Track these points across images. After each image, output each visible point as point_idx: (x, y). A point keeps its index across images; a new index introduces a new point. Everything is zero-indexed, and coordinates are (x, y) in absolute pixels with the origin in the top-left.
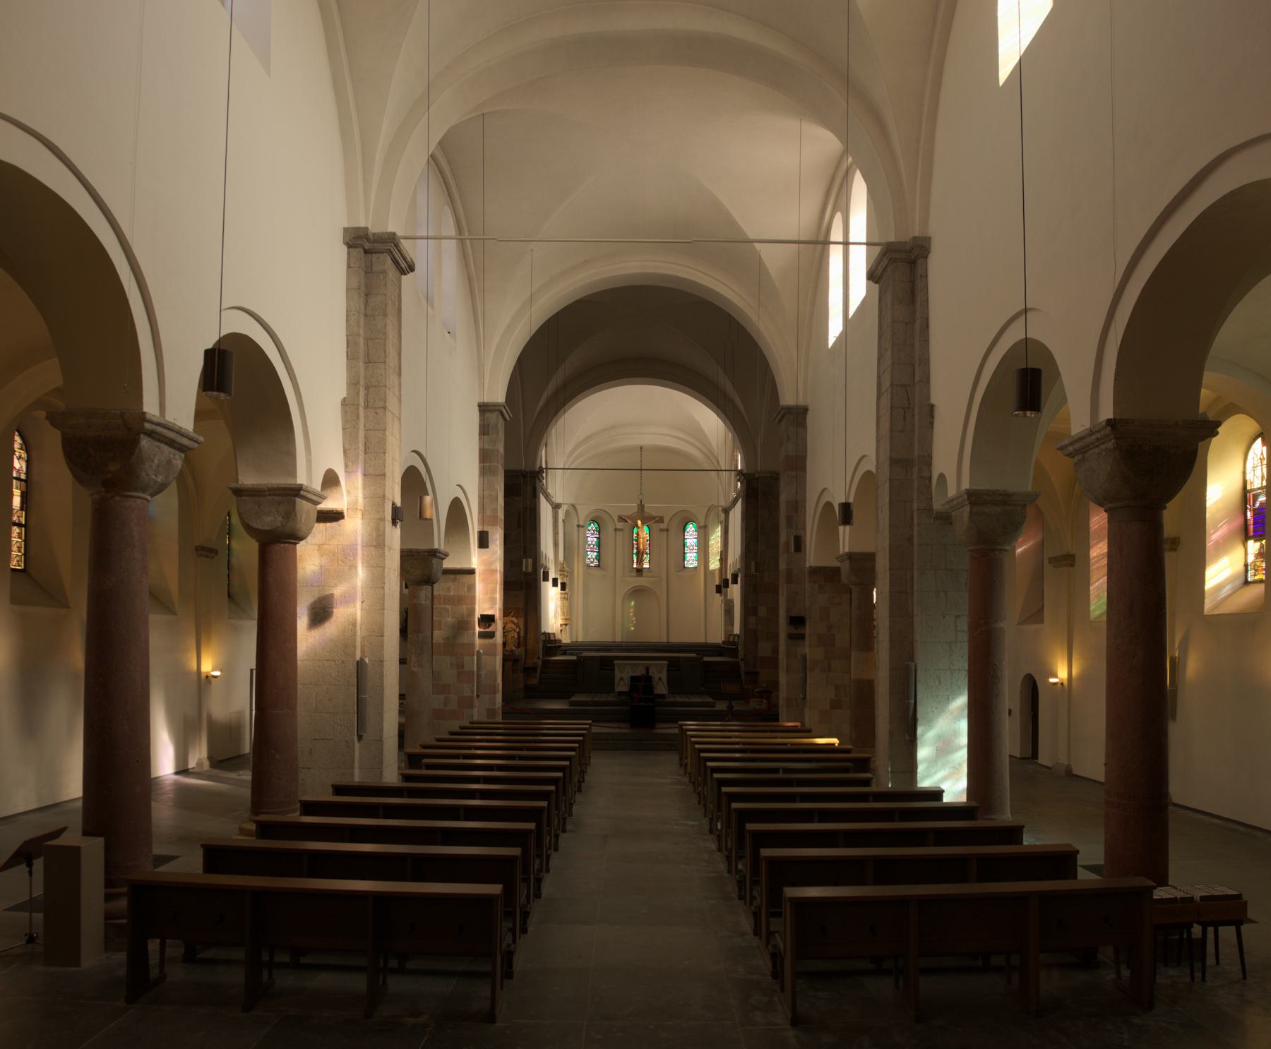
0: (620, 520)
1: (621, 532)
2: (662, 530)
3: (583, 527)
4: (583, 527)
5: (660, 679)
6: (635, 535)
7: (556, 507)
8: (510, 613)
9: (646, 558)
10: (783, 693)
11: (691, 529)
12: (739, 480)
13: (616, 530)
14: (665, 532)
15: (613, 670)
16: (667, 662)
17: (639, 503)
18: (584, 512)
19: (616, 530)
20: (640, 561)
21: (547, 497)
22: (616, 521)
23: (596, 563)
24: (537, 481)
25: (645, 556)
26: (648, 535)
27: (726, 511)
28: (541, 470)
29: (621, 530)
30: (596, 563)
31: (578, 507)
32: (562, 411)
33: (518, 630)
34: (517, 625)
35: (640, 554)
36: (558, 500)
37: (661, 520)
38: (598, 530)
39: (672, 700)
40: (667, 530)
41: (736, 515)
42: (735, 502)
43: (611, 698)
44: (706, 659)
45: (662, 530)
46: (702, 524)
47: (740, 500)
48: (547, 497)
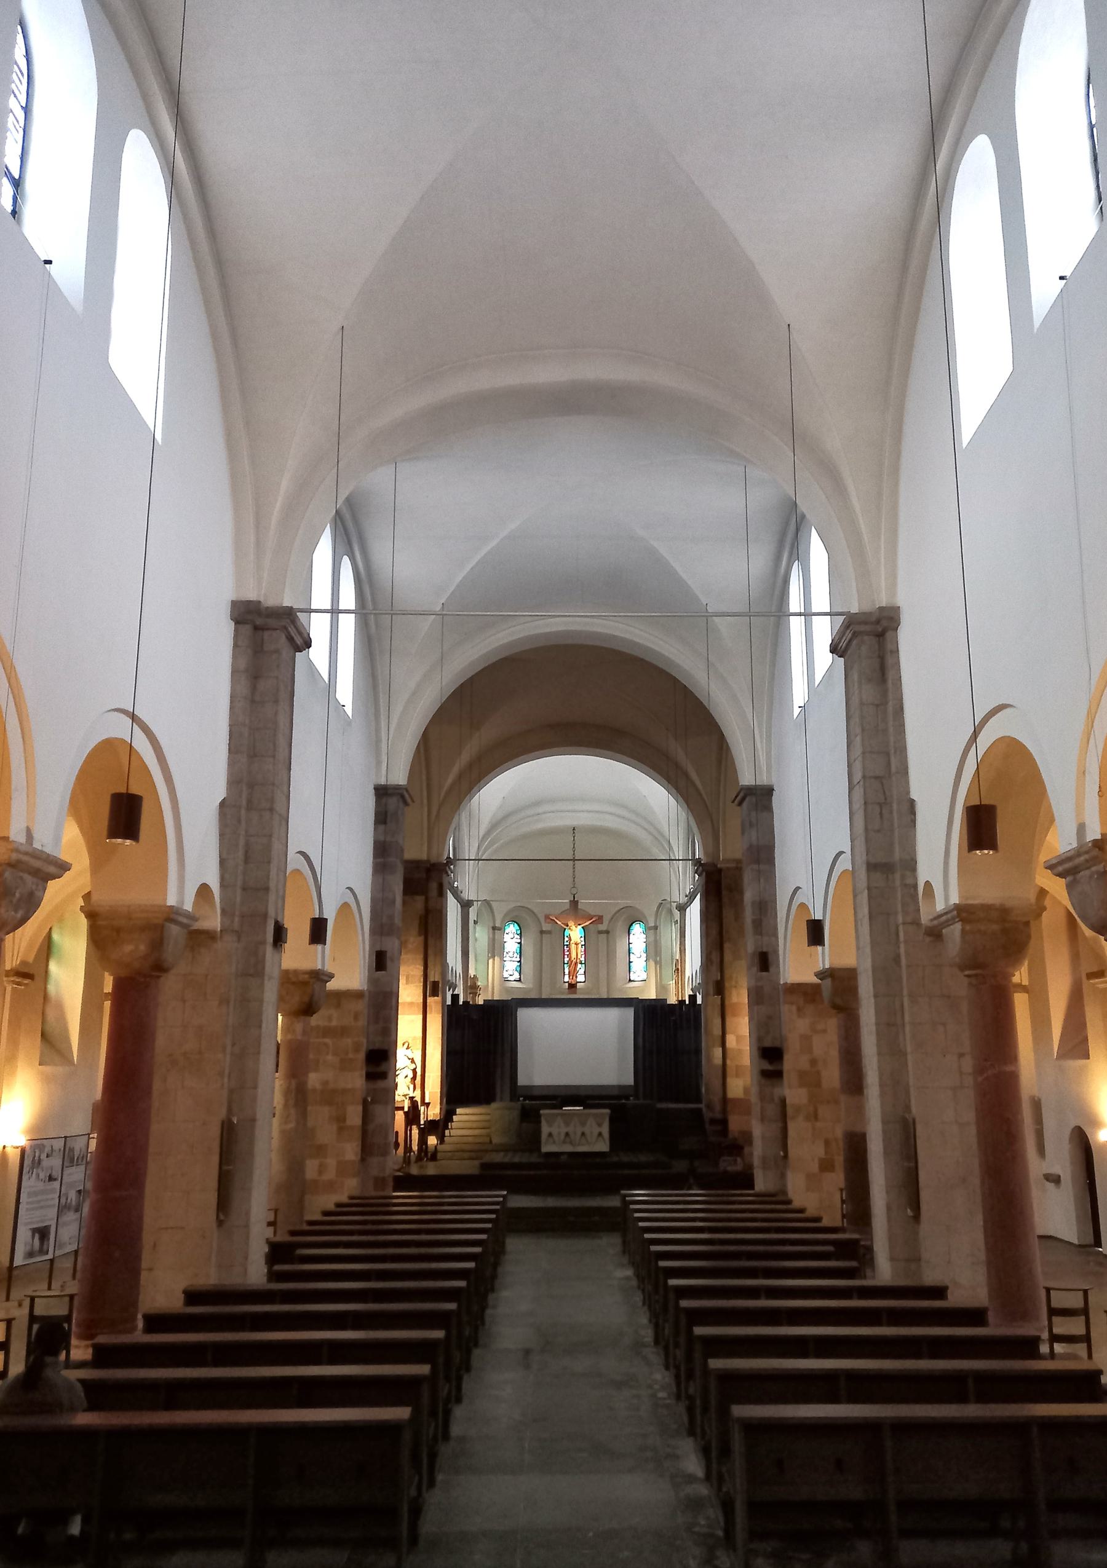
0: (548, 920)
1: (549, 935)
2: (600, 932)
3: (499, 929)
4: (499, 929)
5: (600, 1134)
6: (566, 939)
7: (466, 905)
8: (403, 1045)
9: (581, 969)
10: (758, 1151)
11: (637, 929)
12: (696, 873)
13: (542, 932)
14: (605, 935)
15: (540, 1122)
16: (607, 1111)
17: (572, 899)
18: (500, 910)
19: (542, 932)
20: (573, 973)
21: (456, 894)
22: (542, 920)
23: (516, 976)
24: (444, 876)
25: (579, 966)
26: (583, 939)
27: (682, 908)
28: (450, 862)
29: (549, 932)
30: (516, 976)
31: (494, 904)
32: (476, 788)
33: (413, 1066)
34: (413, 1061)
35: (573, 965)
36: (467, 895)
37: (600, 919)
38: (519, 932)
39: (615, 1159)
40: (607, 932)
41: (694, 911)
42: (691, 898)
43: (534, 1159)
44: (660, 1105)
45: (600, 932)
46: (652, 924)
47: (698, 896)
48: (456, 894)
